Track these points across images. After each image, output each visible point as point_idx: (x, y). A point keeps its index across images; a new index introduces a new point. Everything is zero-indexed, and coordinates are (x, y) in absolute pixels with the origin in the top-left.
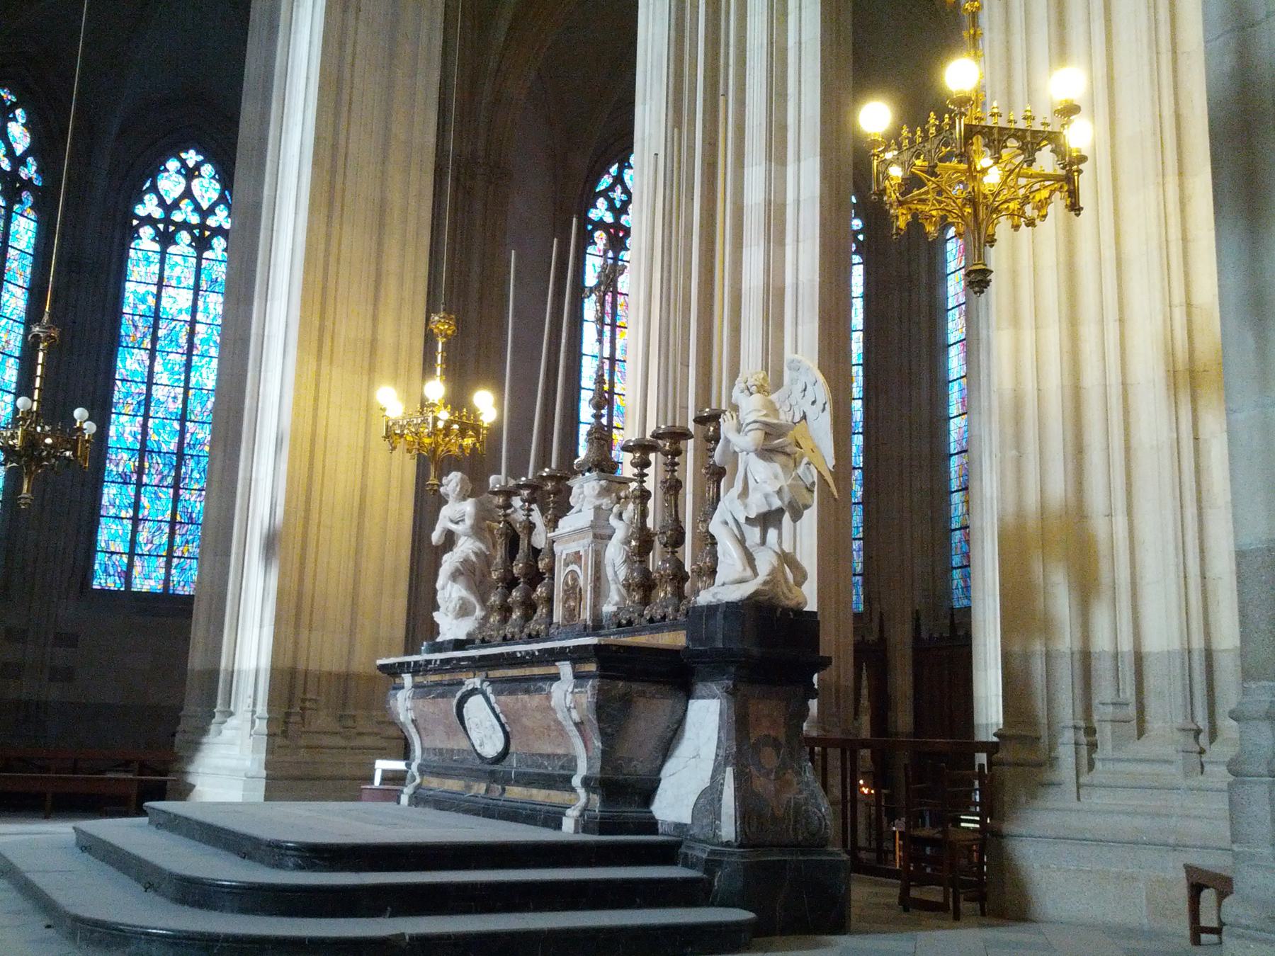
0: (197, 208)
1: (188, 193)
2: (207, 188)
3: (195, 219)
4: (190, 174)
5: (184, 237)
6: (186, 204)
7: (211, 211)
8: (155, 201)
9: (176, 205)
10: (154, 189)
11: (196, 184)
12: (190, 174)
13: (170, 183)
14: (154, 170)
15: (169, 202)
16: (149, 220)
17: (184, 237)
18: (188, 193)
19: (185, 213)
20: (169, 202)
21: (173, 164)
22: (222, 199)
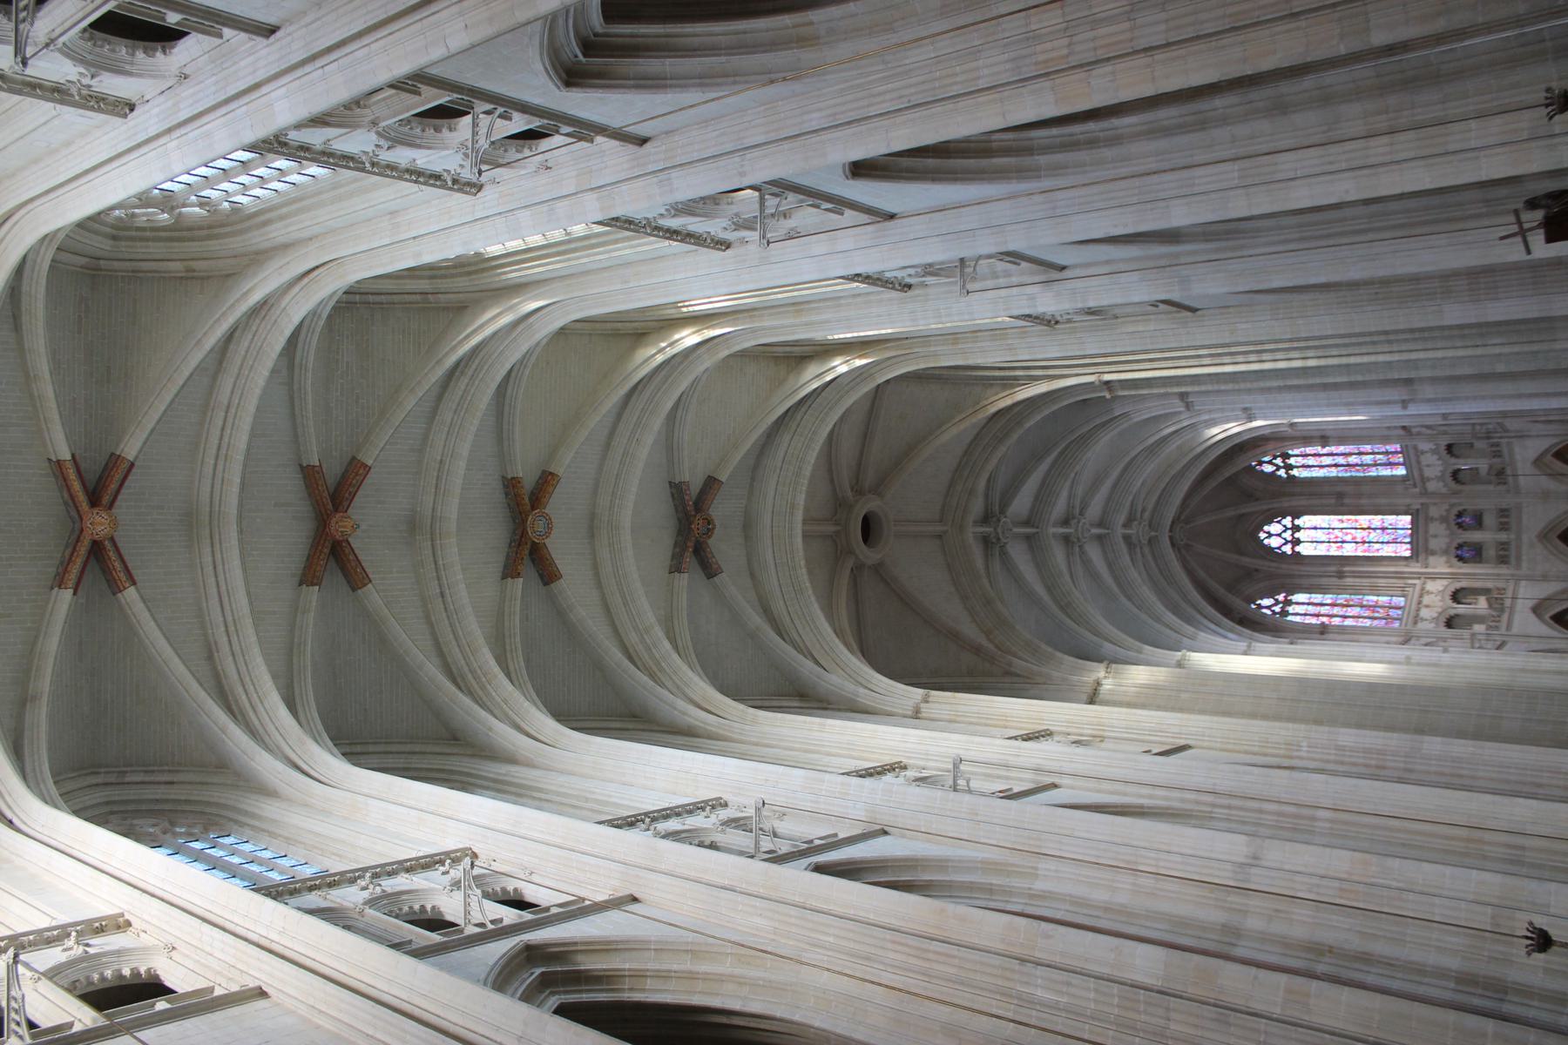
2: (1274, 528)
4: (1270, 535)
12: (1270, 535)
13: (1274, 542)
14: (1270, 549)
19: (1288, 535)
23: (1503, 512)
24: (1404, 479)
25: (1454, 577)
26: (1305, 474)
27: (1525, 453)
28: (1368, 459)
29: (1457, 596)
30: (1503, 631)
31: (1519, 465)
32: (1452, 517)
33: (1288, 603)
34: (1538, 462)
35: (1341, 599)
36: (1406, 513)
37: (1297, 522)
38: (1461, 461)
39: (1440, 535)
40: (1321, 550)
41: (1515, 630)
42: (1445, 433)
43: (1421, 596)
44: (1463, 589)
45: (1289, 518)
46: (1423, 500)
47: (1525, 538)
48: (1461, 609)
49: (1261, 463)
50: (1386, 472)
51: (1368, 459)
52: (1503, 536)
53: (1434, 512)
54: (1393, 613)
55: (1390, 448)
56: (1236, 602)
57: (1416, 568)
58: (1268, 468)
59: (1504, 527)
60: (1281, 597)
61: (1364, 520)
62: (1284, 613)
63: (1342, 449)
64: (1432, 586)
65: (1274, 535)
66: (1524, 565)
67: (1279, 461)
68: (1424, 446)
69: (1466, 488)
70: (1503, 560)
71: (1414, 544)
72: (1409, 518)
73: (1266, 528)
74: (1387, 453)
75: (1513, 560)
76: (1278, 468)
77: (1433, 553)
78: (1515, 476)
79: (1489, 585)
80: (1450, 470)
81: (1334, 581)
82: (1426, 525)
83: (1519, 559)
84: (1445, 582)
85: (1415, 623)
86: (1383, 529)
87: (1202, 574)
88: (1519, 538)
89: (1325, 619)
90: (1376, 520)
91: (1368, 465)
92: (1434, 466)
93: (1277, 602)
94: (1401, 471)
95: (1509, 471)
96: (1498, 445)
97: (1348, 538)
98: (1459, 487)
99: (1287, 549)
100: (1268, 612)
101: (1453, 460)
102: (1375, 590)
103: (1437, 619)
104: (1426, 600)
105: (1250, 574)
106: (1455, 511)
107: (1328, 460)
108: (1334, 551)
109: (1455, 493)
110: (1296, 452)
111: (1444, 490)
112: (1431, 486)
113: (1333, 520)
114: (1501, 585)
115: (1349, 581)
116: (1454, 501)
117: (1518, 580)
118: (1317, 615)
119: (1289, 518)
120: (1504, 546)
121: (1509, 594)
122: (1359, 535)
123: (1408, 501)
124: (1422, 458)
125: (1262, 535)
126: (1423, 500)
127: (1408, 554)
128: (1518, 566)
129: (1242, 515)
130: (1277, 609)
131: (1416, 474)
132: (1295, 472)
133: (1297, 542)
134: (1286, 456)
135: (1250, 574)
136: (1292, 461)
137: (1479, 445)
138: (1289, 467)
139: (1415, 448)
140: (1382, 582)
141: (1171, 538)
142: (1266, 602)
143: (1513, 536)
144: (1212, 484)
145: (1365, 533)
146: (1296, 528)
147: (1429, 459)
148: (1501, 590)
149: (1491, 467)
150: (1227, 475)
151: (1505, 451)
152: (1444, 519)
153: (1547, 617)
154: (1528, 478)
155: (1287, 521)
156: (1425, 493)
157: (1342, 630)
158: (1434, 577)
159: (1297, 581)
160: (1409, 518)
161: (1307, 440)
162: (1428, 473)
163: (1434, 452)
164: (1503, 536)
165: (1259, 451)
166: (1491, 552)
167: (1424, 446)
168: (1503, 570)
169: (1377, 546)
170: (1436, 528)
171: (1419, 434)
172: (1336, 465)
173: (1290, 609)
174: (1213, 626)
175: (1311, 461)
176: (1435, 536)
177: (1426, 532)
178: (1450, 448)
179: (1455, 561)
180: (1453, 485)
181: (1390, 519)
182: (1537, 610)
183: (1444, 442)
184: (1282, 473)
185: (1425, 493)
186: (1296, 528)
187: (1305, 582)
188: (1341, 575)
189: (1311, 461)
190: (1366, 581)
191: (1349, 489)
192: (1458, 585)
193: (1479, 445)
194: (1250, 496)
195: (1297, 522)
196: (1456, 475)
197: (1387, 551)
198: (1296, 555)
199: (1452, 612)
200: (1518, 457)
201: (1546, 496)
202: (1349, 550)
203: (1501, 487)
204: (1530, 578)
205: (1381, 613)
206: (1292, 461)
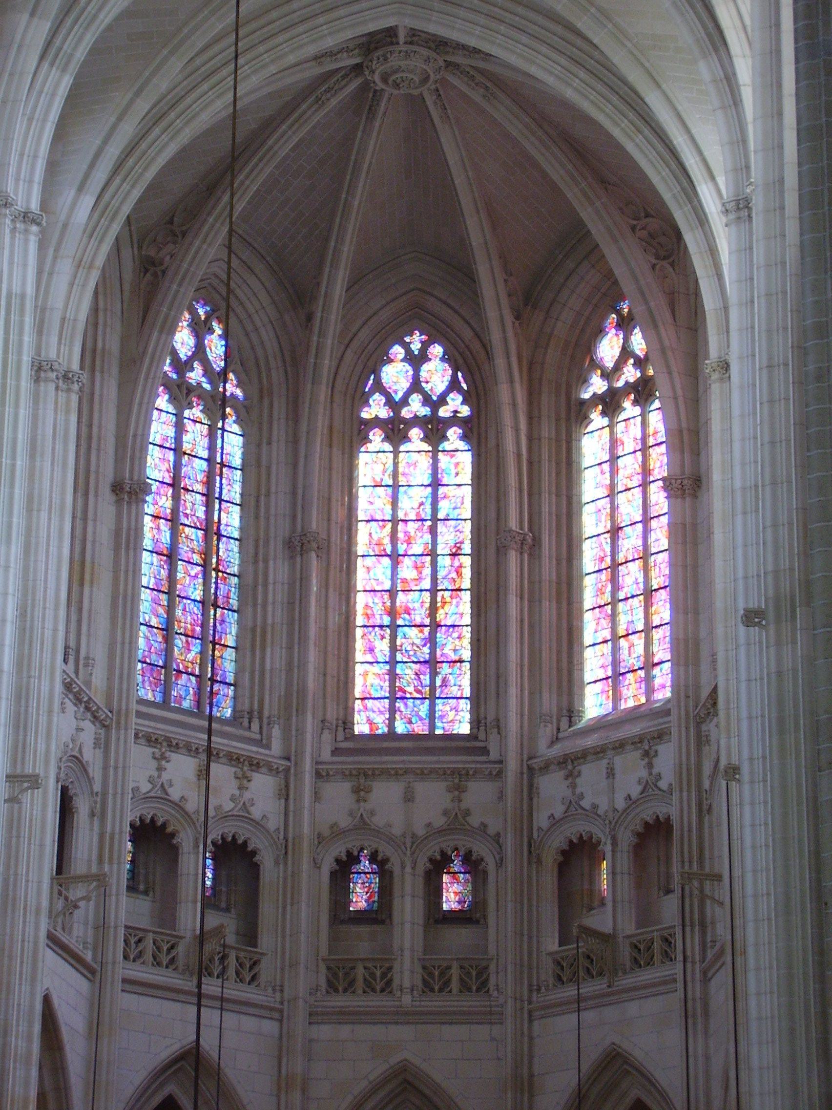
0: (426, 400)
1: (416, 386)
2: (437, 374)
3: (425, 411)
4: (416, 360)
5: (415, 433)
6: (416, 400)
7: (442, 400)
8: (384, 400)
9: (405, 401)
10: (379, 387)
11: (425, 367)
12: (416, 360)
13: (395, 375)
15: (397, 397)
16: (376, 422)
17: (415, 433)
18: (416, 386)
19: (416, 407)
20: (397, 397)
21: (398, 351)
22: (454, 385)
23: (477, 978)
24: (571, 711)
25: (286, 848)
26: (592, 445)
27: (645, 1026)
28: (631, 615)
29: (233, 855)
30: (122, 970)
31: (610, 1013)
32: (464, 842)
33: (217, 405)
34: (615, 1064)
35: (230, 553)
36: (476, 723)
37: (453, 433)
38: (625, 861)
39: (403, 810)
40: (370, 501)
41: (129, 1001)
42: (704, 810)
43: (234, 759)
44: (255, 869)
45: (465, 411)
46: (512, 765)
47: (404, 1032)
48: (198, 871)
49: (625, 325)
50: (594, 664)
51: (631, 615)
52: (407, 973)
53: (479, 794)
54: (185, 690)
55: (663, 676)
56: (206, 252)
57: (314, 746)
58: (608, 349)
59: (434, 980)
60: (232, 388)
61: (459, 610)
62: (182, 393)
63: (660, 538)
64: (262, 789)
65: (416, 373)
66: (324, 1031)
67: (630, 374)
68: (667, 759)
69: (549, 880)
70: (339, 977)
71: (387, 742)
72: (465, 729)
73: (437, 350)
74: (649, 664)
75: (339, 1001)
76: (606, 375)
77: (360, 792)
78: (579, 1004)
79: (266, 941)
80: (599, 832)
81: (280, 529)
82: (443, 774)
83: (344, 1016)
84: (274, 823)
85: (151, 740)
86: (432, 664)
87: (284, 144)
88: (402, 1017)
89: (159, 501)
90: (458, 645)
91: (613, 618)
92: (610, 791)
93: (218, 377)
94: (594, 704)
95: (589, 988)
96: (668, 956)
97: (407, 571)
98: (550, 858)
99: (376, 409)
100: (183, 340)
101: (626, 839)
102: (252, 641)
103: (165, 798)
104: (221, 772)
105: (299, 296)
106: (481, 849)
107: (629, 507)
108: (364, 535)
109: (532, 851)
110: (656, 420)
111: (541, 820)
112: (553, 787)
113: (458, 532)
114: (266, 970)
115: (279, 571)
116: (509, 843)
117: (278, 1014)
118: (176, 484)
119: (465, 411)
120: (382, 981)
121: (234, 990)
122: (416, 603)
123: (513, 724)
124: (633, 756)
125: (416, 342)
126: (512, 765)
127: (361, 727)
128: (315, 1017)
129: (464, 274)
130: (196, 375)
131: (590, 741)
132: (597, 419)
133: (396, 431)
134: (642, 392)
135: (299, 296)
136: (630, 409)
137: (669, 909)
138: (610, 403)
139: (661, 736)
140: (275, 658)
141: (391, 33)
142: (216, 347)
143: (407, 999)
144: (556, 167)
145: (420, 616)
146: (435, 430)
147: (630, 774)
148: (249, 971)
149: (606, 938)
150: (586, 214)
151: (646, 976)
152: (457, 821)
153: (171, 1088)
154: (565, 1045)
155: (456, 404)
156: (532, 771)
157: (128, 541)
158: (284, 793)
159: (279, 431)
160: (465, 729)
161: (689, 439)
162: (591, 775)
163: (650, 786)
164: (407, 973)
165: (658, 302)
166: (362, 944)
167: (667, 759)
168: (306, 980)
169: (383, 647)
170: (432, 801)
171: (702, 740)
172: (615, 531)
173: (196, 412)
174: (113, 151)
175: (629, 465)
176: (409, 798)
177: (423, 774)
178: (657, 831)
179: (339, 850)
180: (558, 841)
181: (461, 682)
182: (192, 1062)
183: (672, 809)
184: (597, 385)
185: (532, 771)
186: (435, 430)
187: (278, 452)
188: (298, 545)
189: (629, 465)
190: (276, 615)
191: (548, 569)
192: (267, 860)
193: (669, 909)
194: (531, 297)
195: (453, 433)
196: (579, 854)
197: (368, 678)
198: (360, 432)
199: (186, 839)
200: (633, 1008)
201: (524, 1085)
202: (370, 573)
203: (547, 972)
204: (281, 1049)
205: (188, 654)
206: (630, 409)
